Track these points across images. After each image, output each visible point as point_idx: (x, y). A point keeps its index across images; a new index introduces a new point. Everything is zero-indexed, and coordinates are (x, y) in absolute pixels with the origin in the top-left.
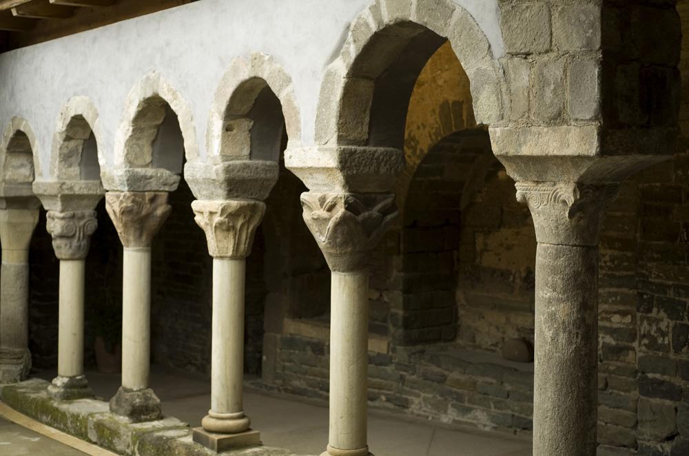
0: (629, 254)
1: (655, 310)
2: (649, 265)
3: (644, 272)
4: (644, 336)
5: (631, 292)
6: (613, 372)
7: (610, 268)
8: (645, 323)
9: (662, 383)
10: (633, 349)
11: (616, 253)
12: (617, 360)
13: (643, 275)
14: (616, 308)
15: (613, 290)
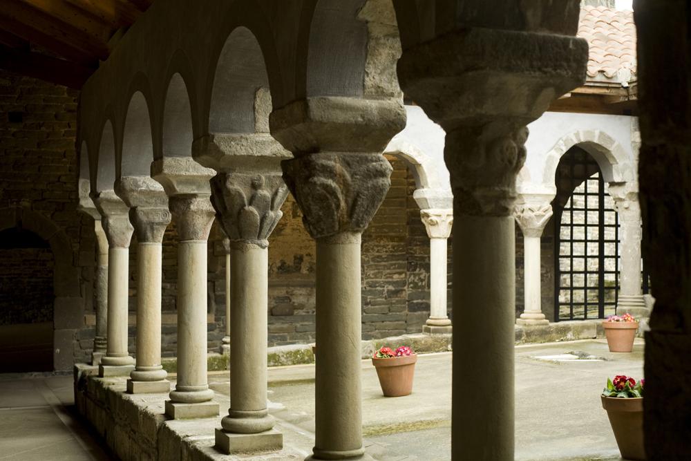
0: (402, 244)
1: (418, 269)
2: (415, 248)
3: (412, 252)
4: (411, 283)
5: (404, 262)
6: (394, 304)
7: (391, 252)
8: (412, 277)
9: (422, 304)
10: (405, 290)
11: (396, 244)
12: (397, 297)
13: (412, 253)
14: (394, 271)
15: (394, 262)
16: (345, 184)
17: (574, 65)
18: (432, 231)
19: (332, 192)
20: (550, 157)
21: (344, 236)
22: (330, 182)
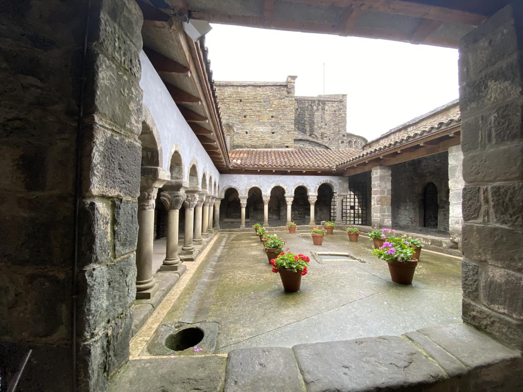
16: (169, 199)
17: (153, 174)
18: (288, 203)
19: (165, 200)
20: (316, 187)
21: (171, 210)
22: (165, 198)
